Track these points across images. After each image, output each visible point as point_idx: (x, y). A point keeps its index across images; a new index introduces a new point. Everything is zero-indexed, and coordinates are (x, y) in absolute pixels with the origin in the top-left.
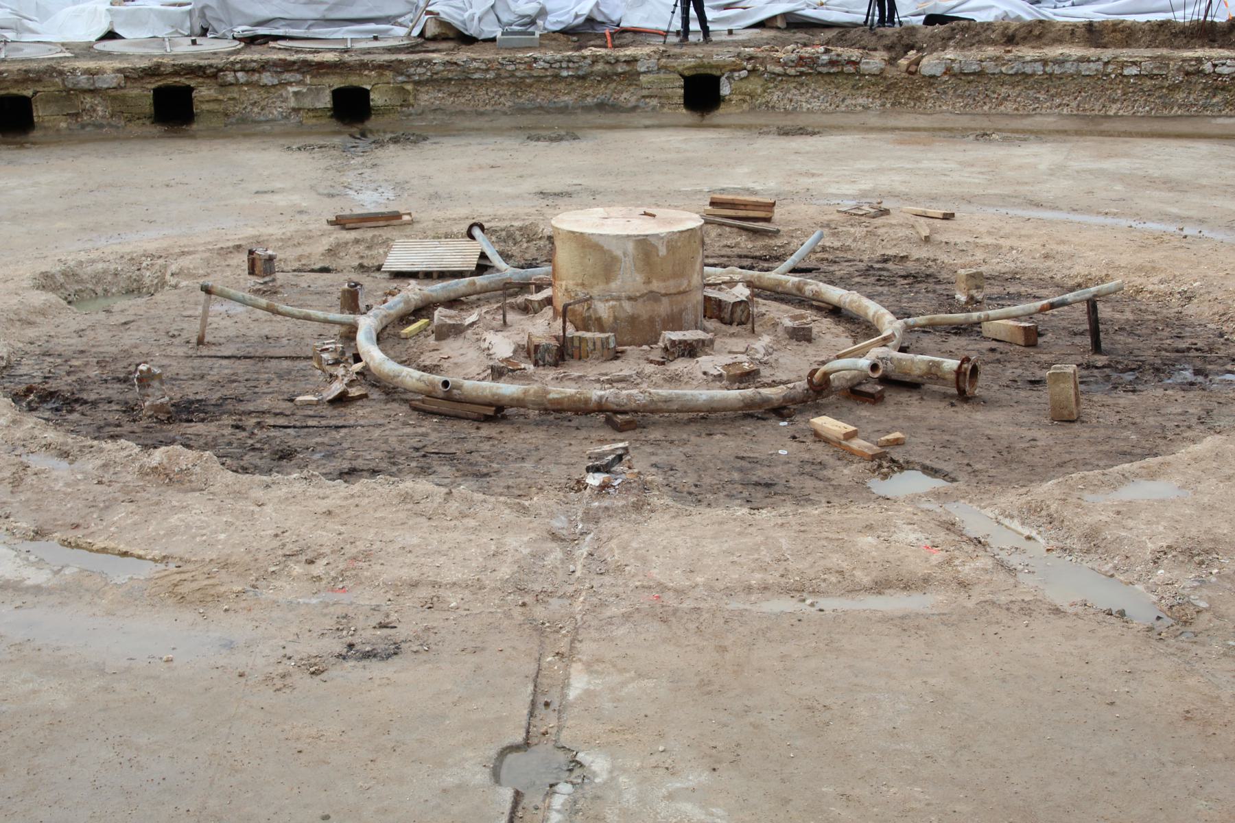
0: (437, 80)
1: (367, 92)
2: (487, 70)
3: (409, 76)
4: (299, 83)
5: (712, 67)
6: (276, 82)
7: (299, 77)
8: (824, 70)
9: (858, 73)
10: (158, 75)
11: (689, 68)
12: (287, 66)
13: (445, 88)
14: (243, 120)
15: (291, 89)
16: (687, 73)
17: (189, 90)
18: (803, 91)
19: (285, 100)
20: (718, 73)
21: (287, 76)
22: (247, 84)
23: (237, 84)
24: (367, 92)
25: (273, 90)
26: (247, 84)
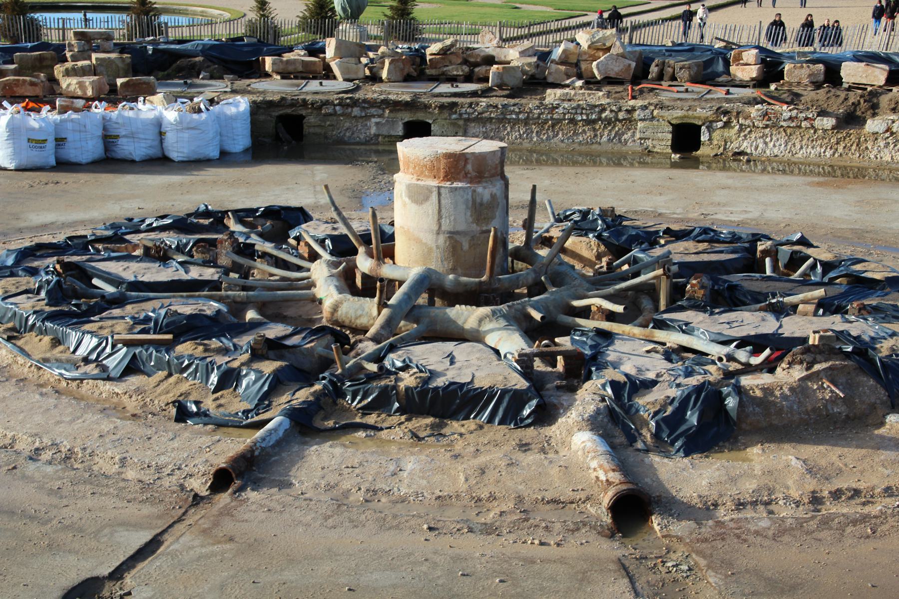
0: (481, 118)
1: (430, 125)
2: (520, 112)
3: (461, 115)
4: (380, 116)
5: (695, 118)
6: (363, 114)
7: (380, 112)
8: (784, 124)
9: (813, 127)
10: (281, 106)
11: (676, 118)
12: (372, 103)
13: (488, 126)
14: (341, 141)
15: (374, 120)
16: (674, 122)
17: (302, 117)
18: (768, 140)
19: (369, 128)
20: (700, 123)
21: (373, 111)
22: (342, 115)
23: (335, 114)
24: (430, 125)
25: (361, 120)
26: (342, 115)
